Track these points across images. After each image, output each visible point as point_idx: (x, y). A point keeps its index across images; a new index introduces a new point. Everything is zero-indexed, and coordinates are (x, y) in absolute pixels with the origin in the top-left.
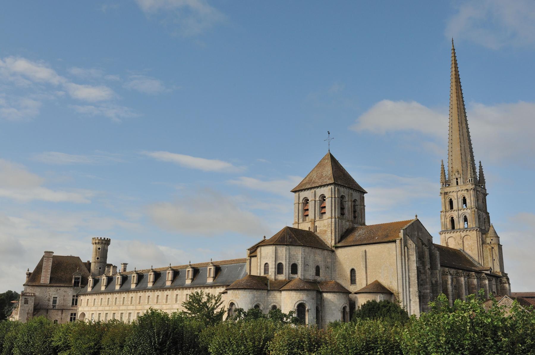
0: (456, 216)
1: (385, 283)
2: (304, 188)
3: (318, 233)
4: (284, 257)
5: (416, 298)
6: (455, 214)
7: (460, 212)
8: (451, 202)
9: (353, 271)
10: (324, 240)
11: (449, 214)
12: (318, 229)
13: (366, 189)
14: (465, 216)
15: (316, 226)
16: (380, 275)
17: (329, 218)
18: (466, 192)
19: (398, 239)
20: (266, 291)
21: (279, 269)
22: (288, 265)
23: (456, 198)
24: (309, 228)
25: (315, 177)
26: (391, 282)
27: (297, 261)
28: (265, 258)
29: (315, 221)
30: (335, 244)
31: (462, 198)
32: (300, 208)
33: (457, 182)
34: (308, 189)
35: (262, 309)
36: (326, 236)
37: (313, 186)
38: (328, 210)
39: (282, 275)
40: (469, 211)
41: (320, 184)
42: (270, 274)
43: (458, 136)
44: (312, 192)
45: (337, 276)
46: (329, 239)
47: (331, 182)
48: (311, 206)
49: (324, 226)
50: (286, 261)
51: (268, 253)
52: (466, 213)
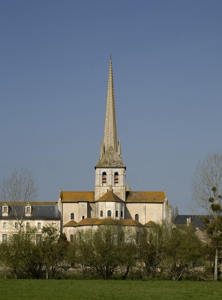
2: (104, 166)
9: (137, 216)
12: (114, 191)
22: (120, 212)
25: (108, 160)
29: (112, 187)
32: (101, 177)
34: (107, 167)
41: (116, 166)
42: (112, 216)
43: (112, 125)
44: (111, 170)
49: (118, 190)
50: (120, 210)
51: (110, 205)
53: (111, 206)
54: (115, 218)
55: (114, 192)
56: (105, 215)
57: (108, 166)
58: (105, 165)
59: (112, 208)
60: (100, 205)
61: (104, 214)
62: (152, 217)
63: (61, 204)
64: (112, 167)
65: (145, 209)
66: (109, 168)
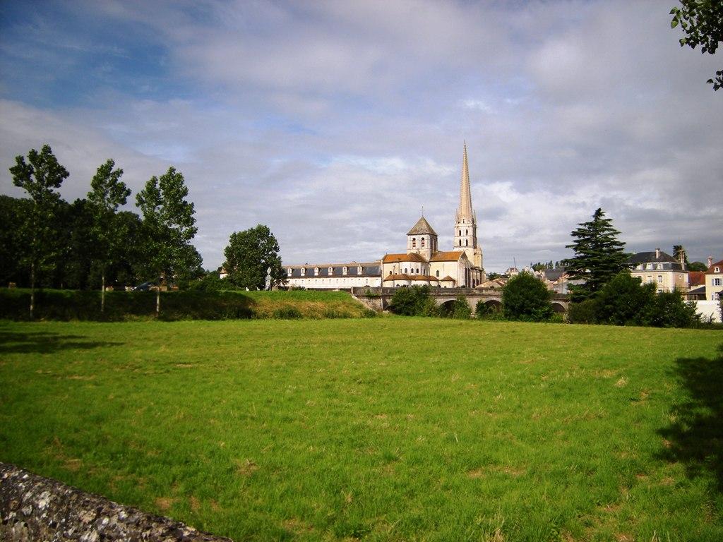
1: (452, 277)
6: (462, 238)
8: (460, 231)
9: (438, 271)
21: (412, 271)
38: (426, 244)
46: (427, 258)
48: (417, 242)
56: (403, 272)
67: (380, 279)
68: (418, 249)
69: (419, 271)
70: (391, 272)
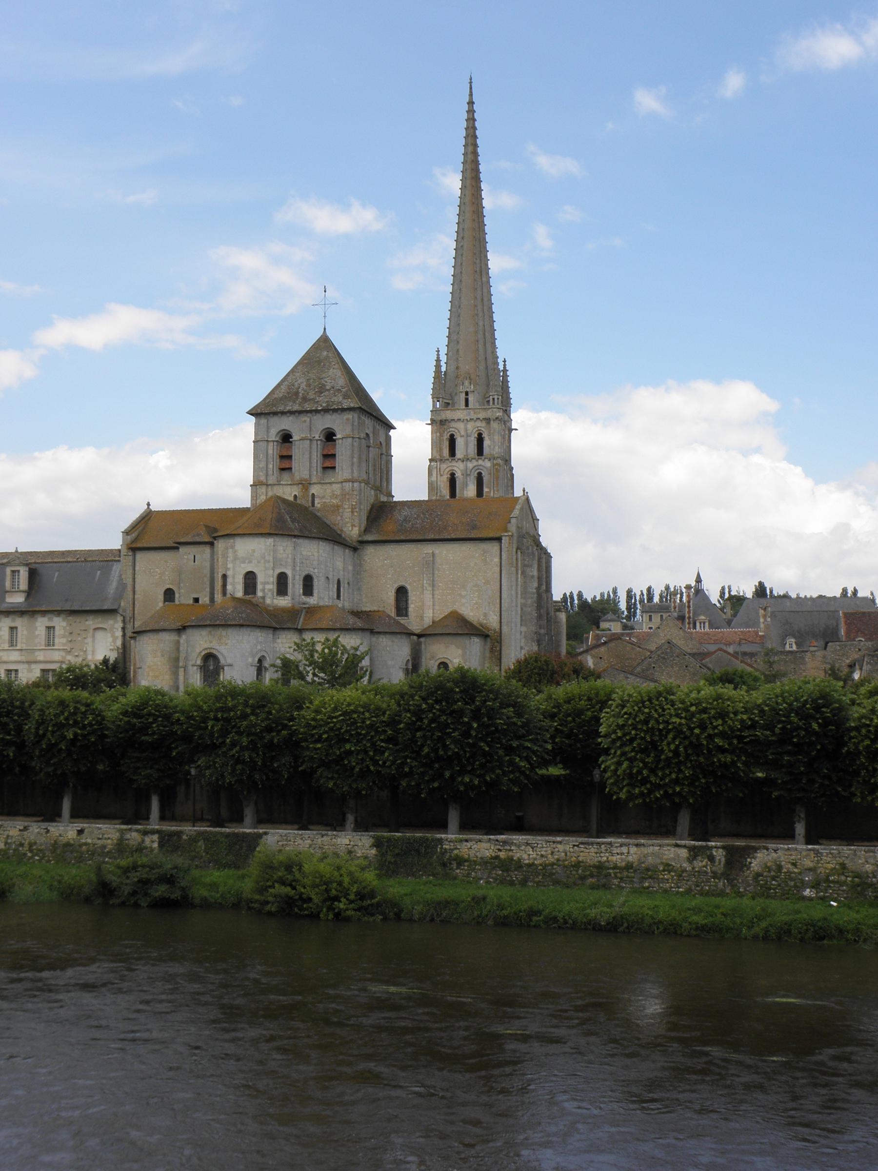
0: (461, 471)
2: (281, 408)
3: (319, 510)
4: (289, 560)
5: (533, 644)
6: (459, 468)
7: (470, 465)
9: (402, 593)
10: (335, 525)
11: (446, 467)
13: (394, 422)
14: (480, 474)
15: (313, 494)
16: (463, 601)
17: (346, 482)
18: (484, 424)
19: (506, 534)
20: (271, 631)
22: (297, 577)
23: (463, 433)
24: (295, 496)
25: (303, 386)
26: (485, 615)
27: (312, 570)
28: (247, 561)
30: (360, 536)
31: (476, 435)
32: (270, 452)
33: (467, 400)
35: (267, 666)
36: (339, 518)
37: (307, 407)
39: (286, 598)
40: (488, 464)
41: (324, 405)
42: (259, 594)
44: (305, 421)
45: (364, 600)
47: (352, 405)
49: (334, 496)
51: (254, 551)
52: (481, 468)
53: (256, 554)
54: (268, 601)
55: (319, 506)
56: (237, 588)
57: (296, 407)
58: (286, 405)
59: (259, 562)
60: (220, 553)
61: (229, 587)
62: (460, 595)
63: (131, 558)
64: (311, 411)
65: (430, 564)
66: (300, 412)
67: (117, 625)
68: (305, 485)
69: (318, 585)
70: (169, 595)
